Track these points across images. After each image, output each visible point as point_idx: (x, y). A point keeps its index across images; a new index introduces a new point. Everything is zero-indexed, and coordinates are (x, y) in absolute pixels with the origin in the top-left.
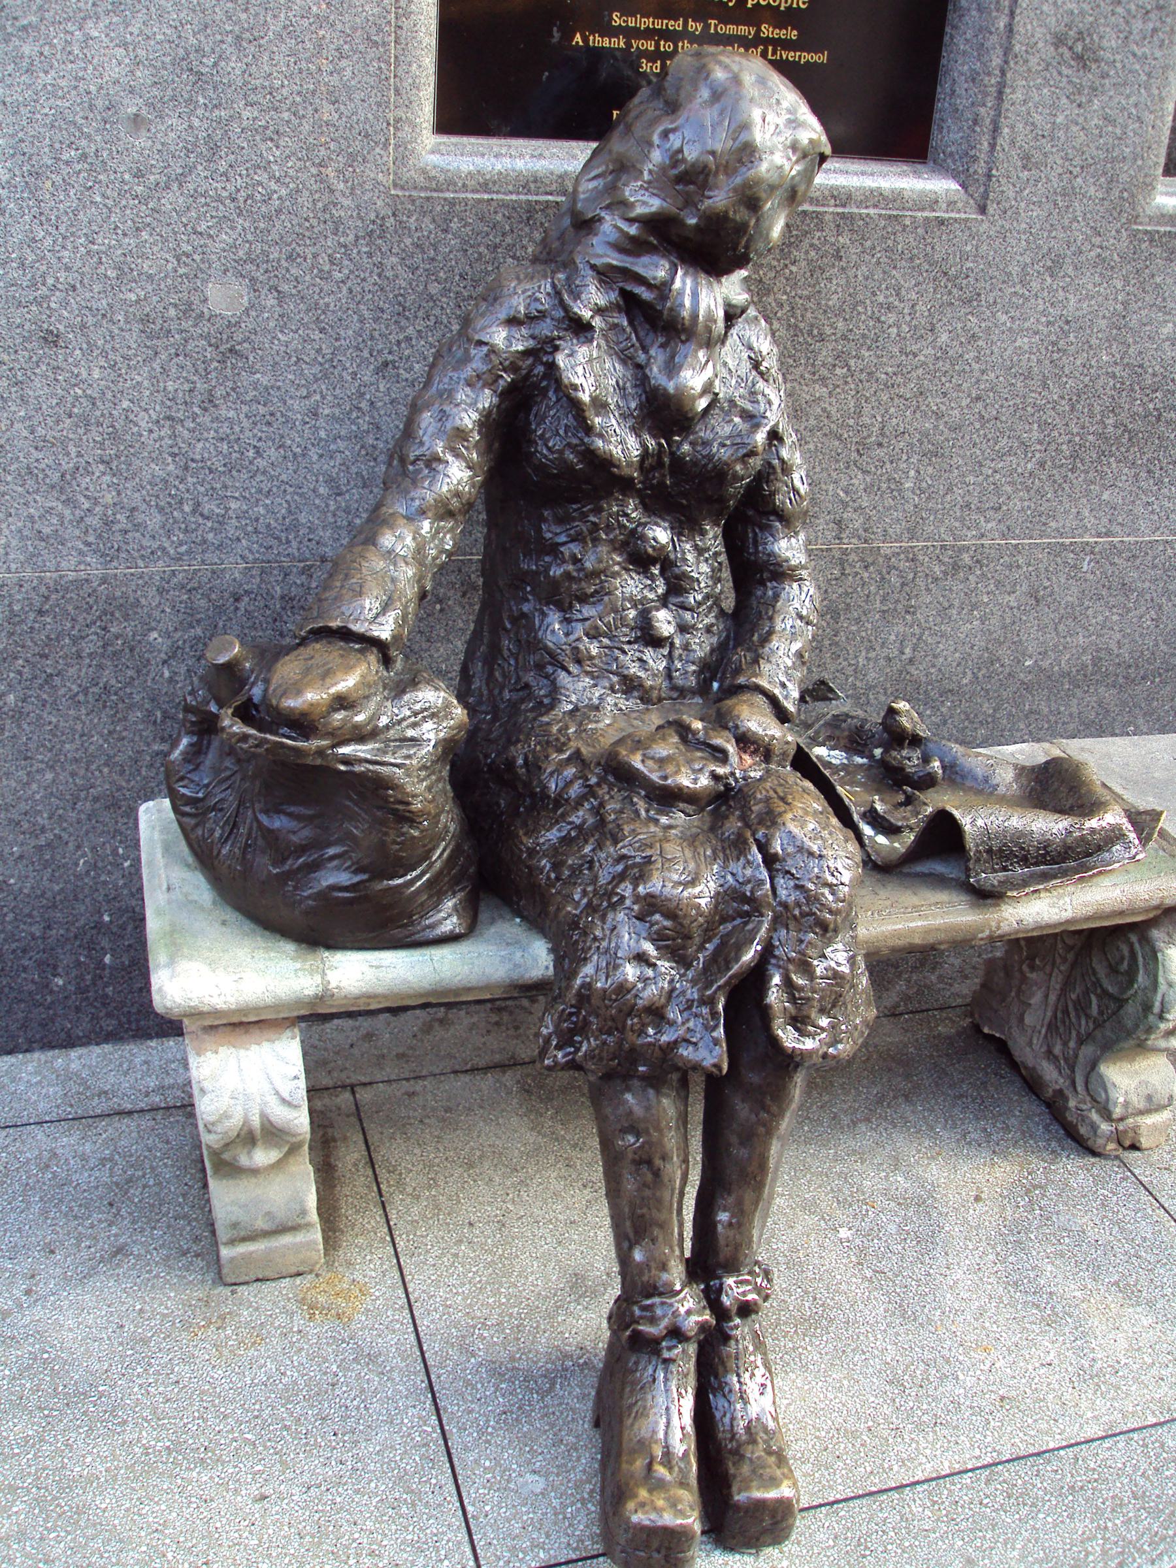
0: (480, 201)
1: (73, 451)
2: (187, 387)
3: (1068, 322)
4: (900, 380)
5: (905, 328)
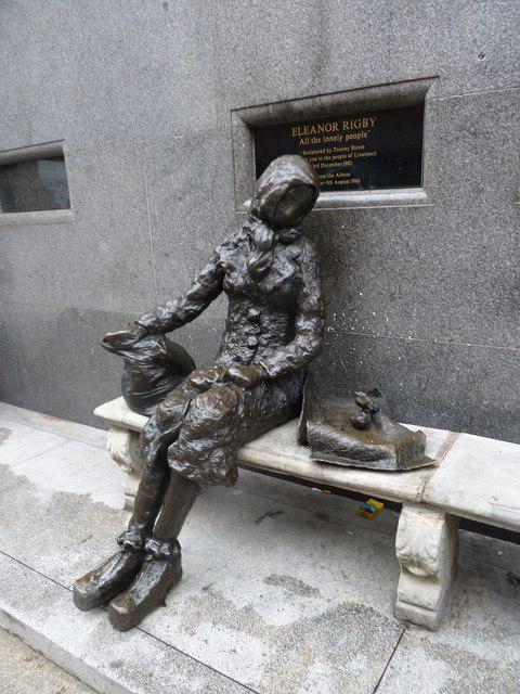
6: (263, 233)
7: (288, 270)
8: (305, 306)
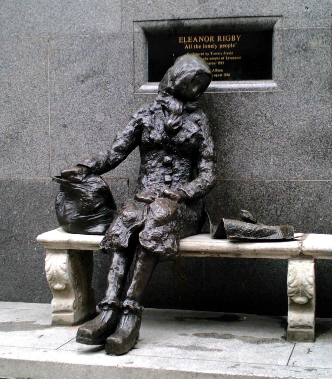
0: (153, 95)
1: (68, 151)
2: (91, 137)
3: (314, 117)
4: (264, 134)
5: (264, 121)
6: (175, 105)
7: (194, 129)
8: (205, 153)
